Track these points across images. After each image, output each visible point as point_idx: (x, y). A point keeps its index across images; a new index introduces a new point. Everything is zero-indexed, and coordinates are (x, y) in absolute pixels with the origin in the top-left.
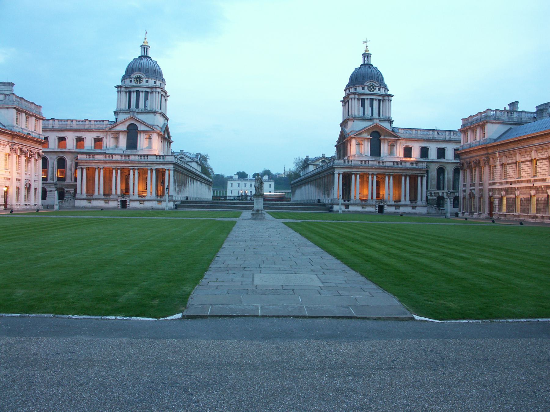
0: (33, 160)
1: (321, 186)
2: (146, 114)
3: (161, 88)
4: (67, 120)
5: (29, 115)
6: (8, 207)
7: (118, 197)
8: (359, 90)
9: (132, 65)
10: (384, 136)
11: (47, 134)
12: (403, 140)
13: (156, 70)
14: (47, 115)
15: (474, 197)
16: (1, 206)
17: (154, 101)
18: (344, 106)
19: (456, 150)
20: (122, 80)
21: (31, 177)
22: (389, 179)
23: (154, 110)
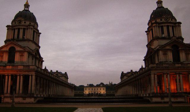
8: (158, 20)
18: (148, 34)
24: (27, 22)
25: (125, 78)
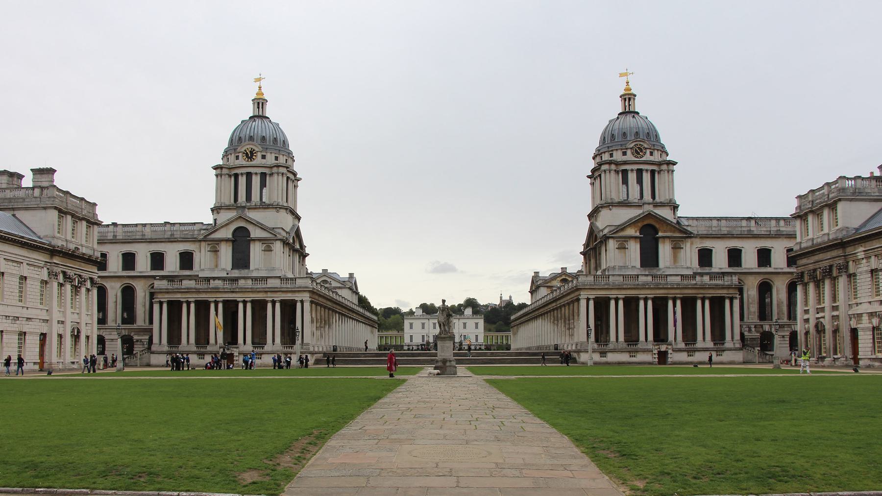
0: (83, 290)
1: (560, 321)
2: (263, 210)
3: (287, 168)
4: (136, 225)
5: (77, 218)
6: (46, 366)
7: (220, 348)
8: (618, 156)
9: (238, 134)
10: (664, 232)
11: (105, 249)
12: (696, 237)
13: (278, 138)
14: (105, 216)
15: (824, 330)
16: (35, 366)
17: (275, 190)
19: (789, 250)
20: (223, 157)
21: (80, 318)
22: (675, 306)
23: (276, 204)
24: (268, 156)
25: (543, 292)
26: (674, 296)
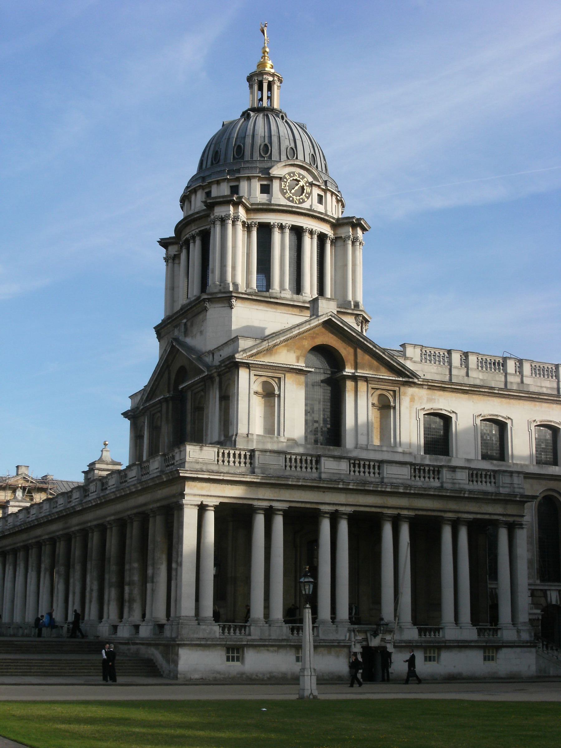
26: (395, 512)
